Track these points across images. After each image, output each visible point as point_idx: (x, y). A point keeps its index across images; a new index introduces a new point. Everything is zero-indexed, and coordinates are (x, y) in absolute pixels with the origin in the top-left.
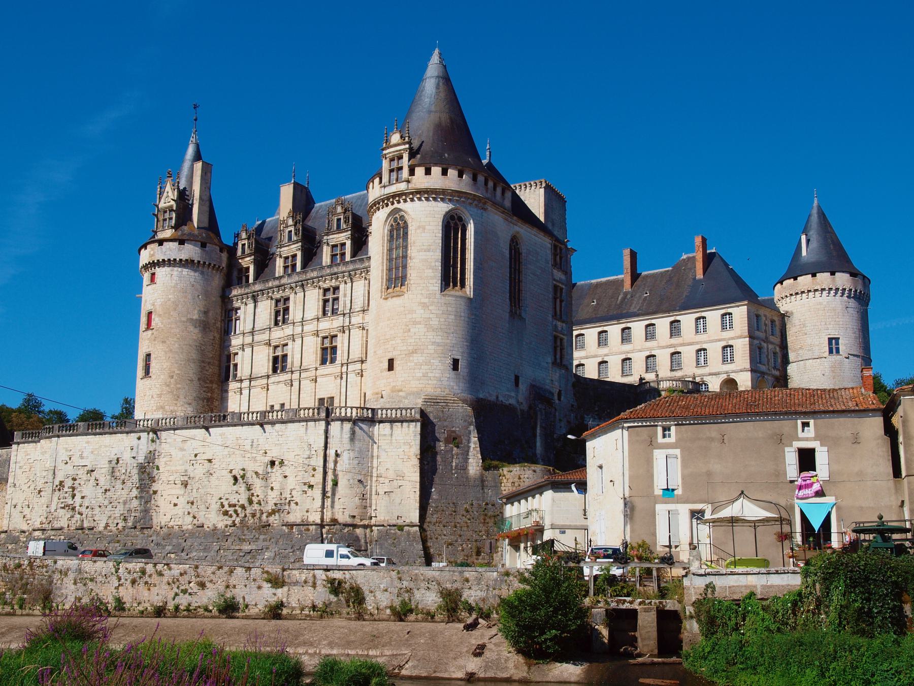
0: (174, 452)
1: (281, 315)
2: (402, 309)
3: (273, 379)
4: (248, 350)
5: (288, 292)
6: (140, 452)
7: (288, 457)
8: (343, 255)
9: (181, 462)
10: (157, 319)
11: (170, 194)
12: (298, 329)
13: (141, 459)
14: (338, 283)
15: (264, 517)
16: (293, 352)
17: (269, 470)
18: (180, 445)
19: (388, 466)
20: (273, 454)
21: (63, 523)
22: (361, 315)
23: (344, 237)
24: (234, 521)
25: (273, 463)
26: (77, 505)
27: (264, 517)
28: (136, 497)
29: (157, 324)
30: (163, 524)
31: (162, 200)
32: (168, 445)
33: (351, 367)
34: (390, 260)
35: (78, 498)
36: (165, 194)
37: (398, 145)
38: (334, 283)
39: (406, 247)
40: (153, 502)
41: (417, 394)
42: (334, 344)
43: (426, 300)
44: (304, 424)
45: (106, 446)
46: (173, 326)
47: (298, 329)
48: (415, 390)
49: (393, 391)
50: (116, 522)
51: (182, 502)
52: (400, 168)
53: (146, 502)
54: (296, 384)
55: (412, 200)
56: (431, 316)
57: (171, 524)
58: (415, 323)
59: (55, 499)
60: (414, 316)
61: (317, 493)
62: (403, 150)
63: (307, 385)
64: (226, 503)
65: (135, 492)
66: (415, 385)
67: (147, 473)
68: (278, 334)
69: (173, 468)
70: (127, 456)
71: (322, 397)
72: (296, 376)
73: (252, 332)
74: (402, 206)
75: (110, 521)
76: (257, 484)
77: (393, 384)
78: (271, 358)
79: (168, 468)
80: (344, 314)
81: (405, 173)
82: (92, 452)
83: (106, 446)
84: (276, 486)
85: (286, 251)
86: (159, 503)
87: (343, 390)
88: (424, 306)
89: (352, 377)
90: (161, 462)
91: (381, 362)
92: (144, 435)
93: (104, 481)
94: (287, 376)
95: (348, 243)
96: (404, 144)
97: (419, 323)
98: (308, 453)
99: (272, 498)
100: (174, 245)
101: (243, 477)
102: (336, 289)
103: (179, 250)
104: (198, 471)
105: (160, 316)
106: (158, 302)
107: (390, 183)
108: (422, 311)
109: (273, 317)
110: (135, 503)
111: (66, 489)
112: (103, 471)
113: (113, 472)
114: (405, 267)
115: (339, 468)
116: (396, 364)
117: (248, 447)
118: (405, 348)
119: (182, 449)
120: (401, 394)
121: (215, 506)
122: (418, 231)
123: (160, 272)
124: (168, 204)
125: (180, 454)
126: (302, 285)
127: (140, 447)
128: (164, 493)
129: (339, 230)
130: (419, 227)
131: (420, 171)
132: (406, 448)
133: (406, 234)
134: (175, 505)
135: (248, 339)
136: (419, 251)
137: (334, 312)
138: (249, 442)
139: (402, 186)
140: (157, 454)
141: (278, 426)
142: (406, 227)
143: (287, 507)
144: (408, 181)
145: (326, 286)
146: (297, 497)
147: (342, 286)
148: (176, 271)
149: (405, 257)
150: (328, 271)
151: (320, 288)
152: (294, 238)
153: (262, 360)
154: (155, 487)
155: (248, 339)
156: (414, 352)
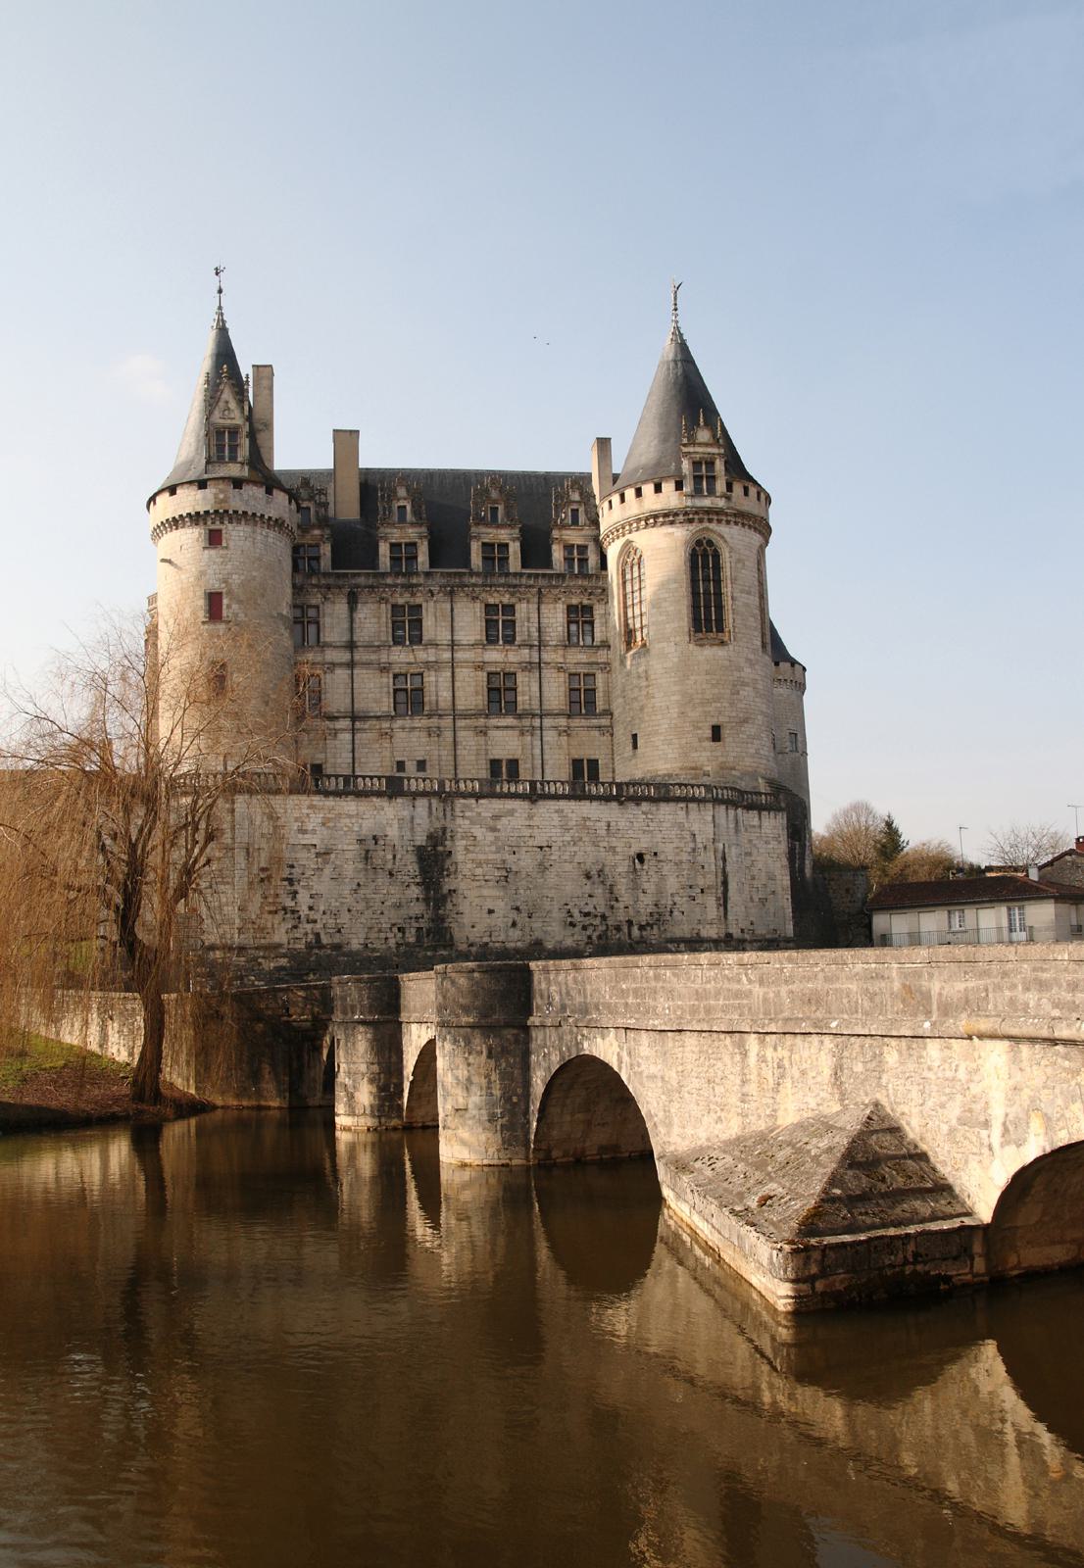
0: (478, 832)
1: (407, 627)
2: (727, 663)
3: (399, 723)
4: (342, 674)
5: (419, 600)
6: (418, 829)
7: (668, 851)
8: (504, 560)
9: (493, 848)
10: (235, 606)
11: (233, 405)
12: (447, 655)
13: (421, 839)
14: (513, 600)
15: (636, 932)
16: (438, 688)
17: (638, 866)
18: (491, 823)
19: (760, 866)
20: (642, 844)
21: (280, 936)
22: (561, 652)
23: (508, 536)
24: (590, 937)
25: (640, 857)
26: (304, 911)
27: (636, 932)
28: (418, 899)
29: (236, 615)
30: (472, 939)
31: (217, 414)
32: (467, 822)
33: (548, 722)
34: (695, 593)
35: (303, 898)
36: (221, 404)
37: (706, 445)
38: (506, 599)
39: (718, 582)
40: (449, 906)
41: (754, 775)
42: (509, 685)
43: (752, 657)
44: (683, 805)
45: (350, 816)
46: (262, 622)
47: (447, 655)
48: (750, 769)
49: (722, 768)
50: (383, 935)
51: (501, 907)
52: (712, 479)
53: (437, 907)
54: (448, 735)
55: (728, 522)
56: (757, 677)
57: (486, 939)
58: (744, 684)
59: (258, 899)
60: (742, 674)
61: (711, 901)
62: (719, 454)
63: (467, 738)
64: (576, 913)
65: (415, 891)
66: (748, 763)
67: (433, 860)
68: (400, 656)
69: (482, 857)
70: (393, 832)
71: (497, 757)
72: (447, 722)
73: (351, 646)
74: (723, 529)
75: (373, 935)
76: (622, 887)
77: (721, 759)
78: (392, 691)
79: (470, 856)
80: (531, 646)
81: (720, 486)
82: (324, 824)
83: (350, 816)
84: (650, 887)
85: (396, 535)
86: (461, 909)
87: (537, 751)
88: (751, 663)
89: (550, 736)
90: (459, 848)
91: (700, 728)
92: (422, 803)
93: (351, 868)
94: (434, 721)
95: (515, 548)
96: (719, 446)
97: (747, 685)
98: (692, 845)
99: (646, 903)
100: (259, 492)
101: (600, 872)
102: (510, 609)
103: (268, 502)
104: (526, 861)
105: (240, 602)
106: (236, 579)
107: (697, 492)
108: (749, 670)
109: (390, 630)
110: (418, 909)
111: (276, 881)
112: (349, 855)
113: (366, 858)
114: (720, 607)
115: (728, 869)
116: (725, 733)
117: (603, 832)
118: (734, 714)
119: (494, 829)
120: (734, 772)
121: (558, 915)
122: (740, 565)
123: (236, 534)
124: (229, 421)
125: (490, 836)
126: (451, 594)
127: (417, 821)
128: (472, 894)
129: (493, 522)
130: (739, 561)
131: (738, 488)
132: (773, 844)
133: (717, 568)
134: (491, 912)
135: (345, 656)
136: (742, 592)
137: (510, 640)
138: (603, 825)
139: (721, 503)
140: (448, 834)
141: (645, 806)
142: (717, 556)
143: (669, 918)
144: (728, 498)
145: (491, 601)
146: (682, 902)
147: (522, 610)
148: (261, 532)
149: (719, 594)
150: (480, 581)
151: (482, 602)
152: (409, 517)
153: (374, 692)
154: (448, 884)
155: (345, 656)
156: (745, 721)
